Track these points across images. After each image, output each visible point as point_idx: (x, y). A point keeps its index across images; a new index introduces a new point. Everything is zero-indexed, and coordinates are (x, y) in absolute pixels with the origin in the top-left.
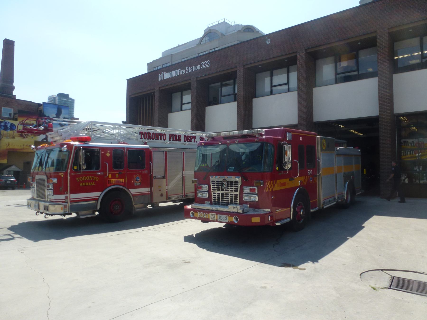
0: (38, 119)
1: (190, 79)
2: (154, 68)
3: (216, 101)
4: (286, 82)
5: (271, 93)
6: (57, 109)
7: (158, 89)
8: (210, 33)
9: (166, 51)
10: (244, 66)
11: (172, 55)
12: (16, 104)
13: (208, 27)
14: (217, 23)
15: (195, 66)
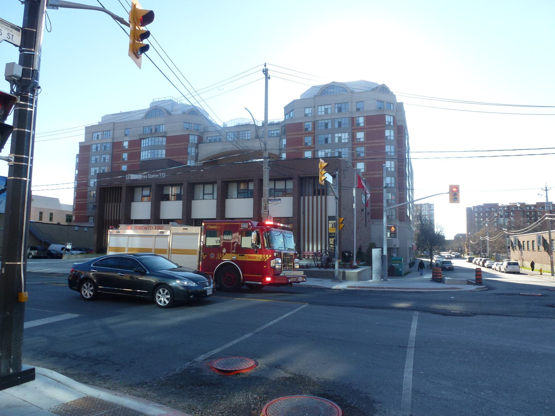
2: (93, 133)
3: (167, 198)
4: (212, 193)
10: (187, 181)
11: (114, 123)
15: (155, 175)
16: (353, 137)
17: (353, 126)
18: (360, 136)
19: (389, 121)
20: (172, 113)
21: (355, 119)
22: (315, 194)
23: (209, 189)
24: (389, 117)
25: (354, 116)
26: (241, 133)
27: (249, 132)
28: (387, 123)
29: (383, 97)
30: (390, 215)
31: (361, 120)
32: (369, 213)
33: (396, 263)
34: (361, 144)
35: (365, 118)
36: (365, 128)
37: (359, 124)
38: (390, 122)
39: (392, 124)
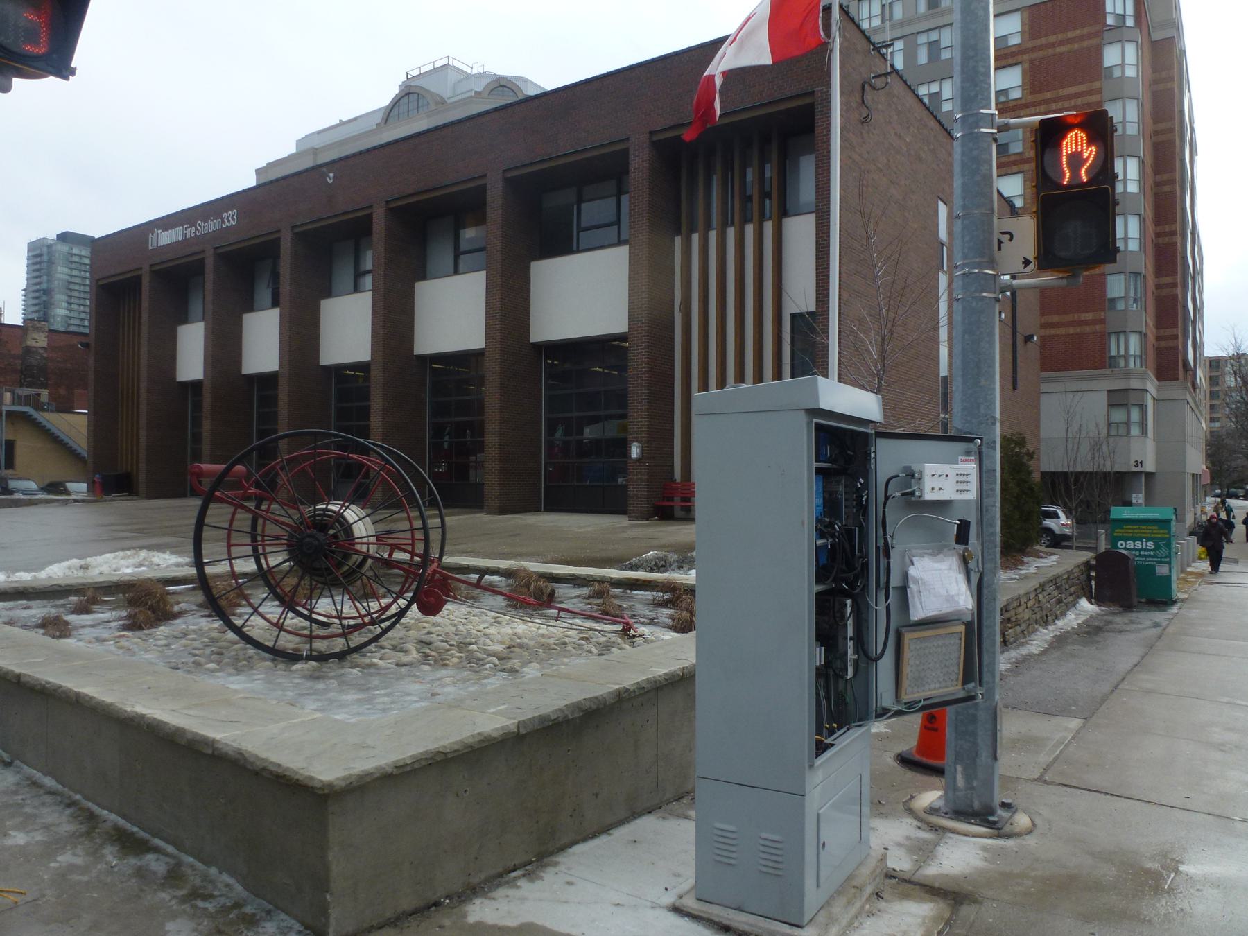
1: (204, 251)
8: (408, 94)
9: (307, 136)
13: (409, 76)
14: (430, 67)
19: (1119, 11)
28: (1110, 21)
30: (1122, 352)
32: (1028, 338)
33: (1140, 539)
36: (1026, 51)
38: (1122, 17)
39: (1130, 22)
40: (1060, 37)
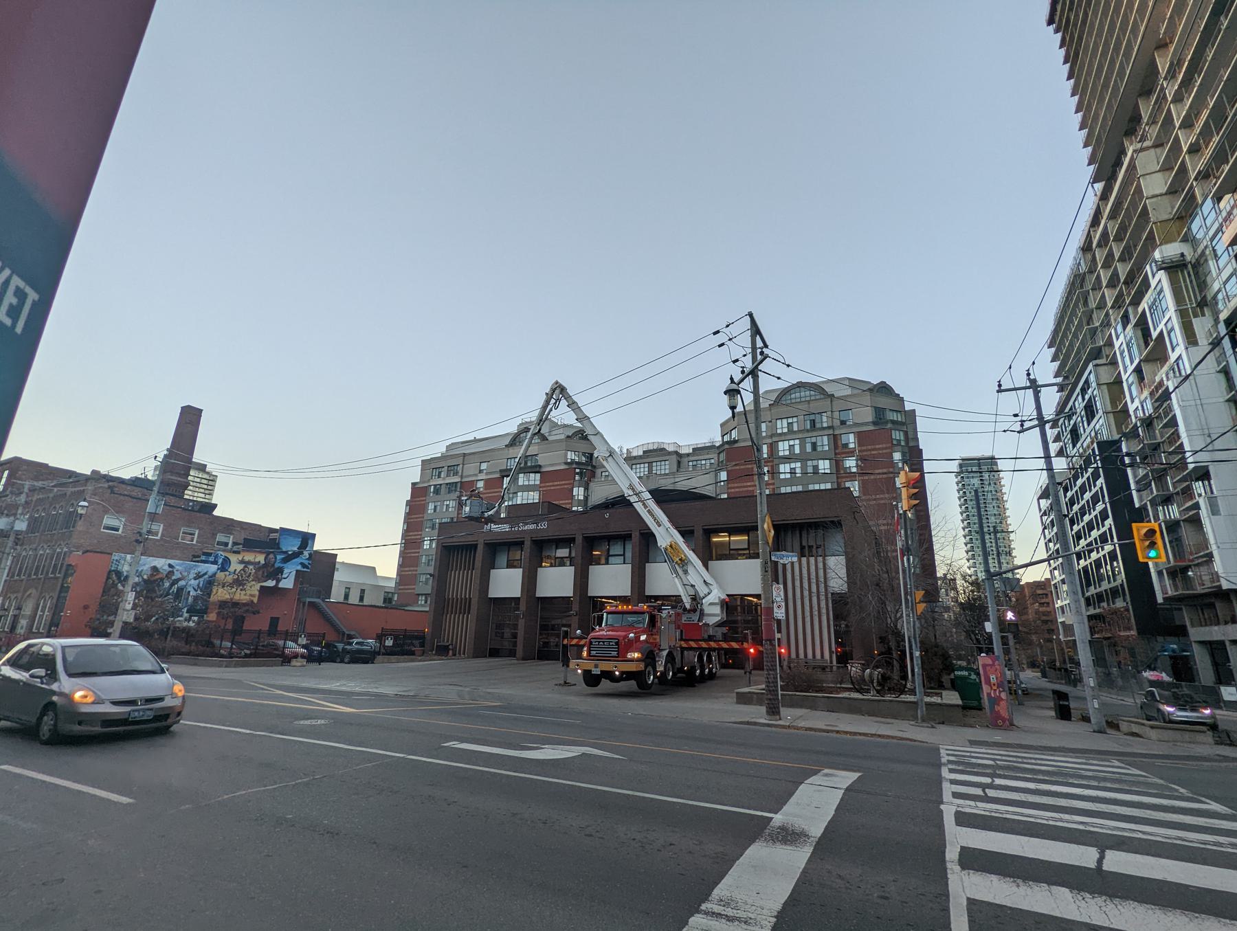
0: (268, 554)
4: (622, 553)
5: (607, 563)
6: (301, 539)
7: (482, 541)
12: (238, 529)
16: (837, 465)
17: (837, 449)
18: (851, 463)
19: (898, 438)
20: (550, 438)
21: (839, 437)
22: (802, 555)
23: (616, 549)
24: (897, 432)
25: (837, 432)
26: (654, 464)
27: (667, 462)
29: (883, 402)
31: (851, 440)
34: (851, 476)
35: (856, 436)
37: (846, 445)
39: (903, 443)
40: (873, 447)
